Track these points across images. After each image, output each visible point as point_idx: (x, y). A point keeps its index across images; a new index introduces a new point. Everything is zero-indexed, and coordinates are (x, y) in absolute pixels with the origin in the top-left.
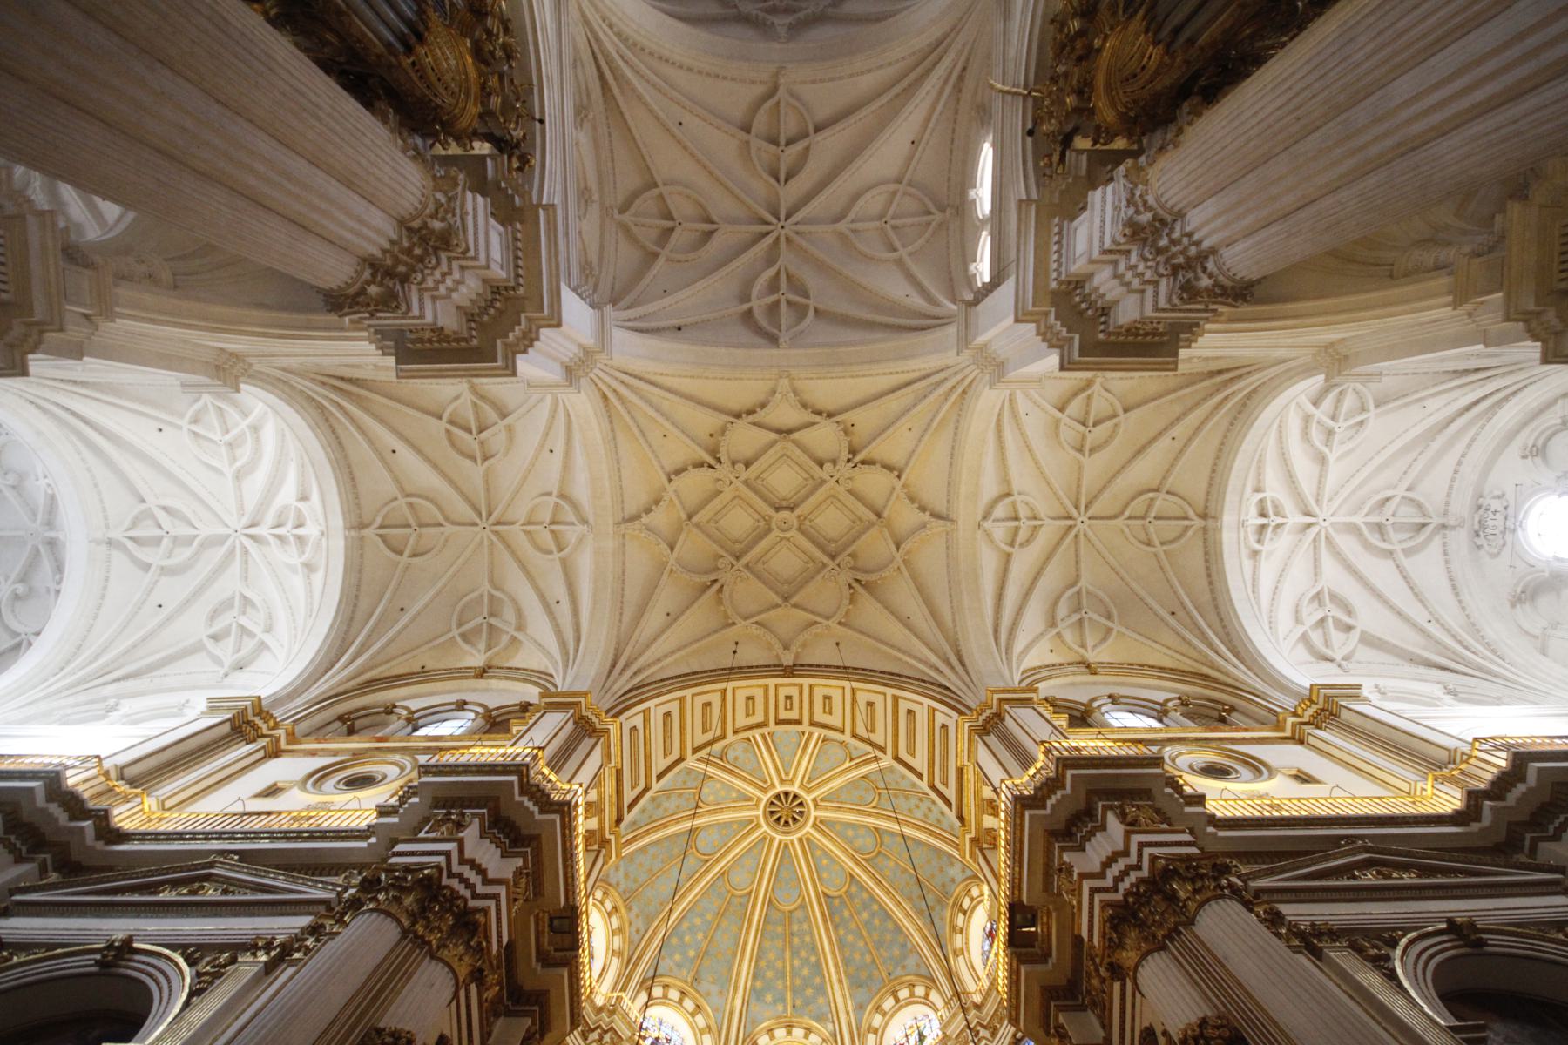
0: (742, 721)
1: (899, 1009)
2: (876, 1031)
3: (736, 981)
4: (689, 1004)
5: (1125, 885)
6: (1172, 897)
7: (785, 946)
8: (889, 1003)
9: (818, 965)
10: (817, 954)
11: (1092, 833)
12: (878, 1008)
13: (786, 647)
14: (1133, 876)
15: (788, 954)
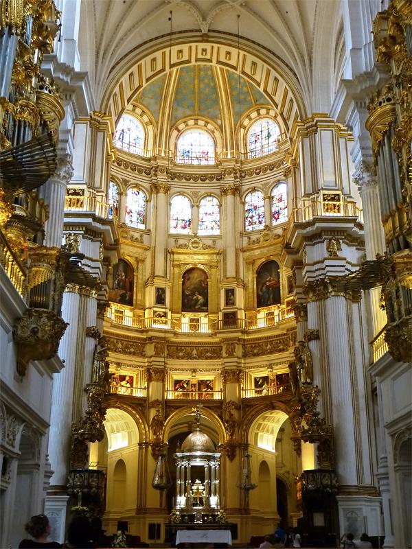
0: (174, 60)
1: (260, 118)
2: (245, 128)
3: (166, 97)
4: (138, 111)
5: (317, 273)
6: (326, 287)
7: (195, 76)
8: (254, 115)
9: (215, 87)
10: (214, 81)
11: (319, 243)
12: (248, 116)
13: (204, 19)
14: (320, 272)
15: (196, 81)
